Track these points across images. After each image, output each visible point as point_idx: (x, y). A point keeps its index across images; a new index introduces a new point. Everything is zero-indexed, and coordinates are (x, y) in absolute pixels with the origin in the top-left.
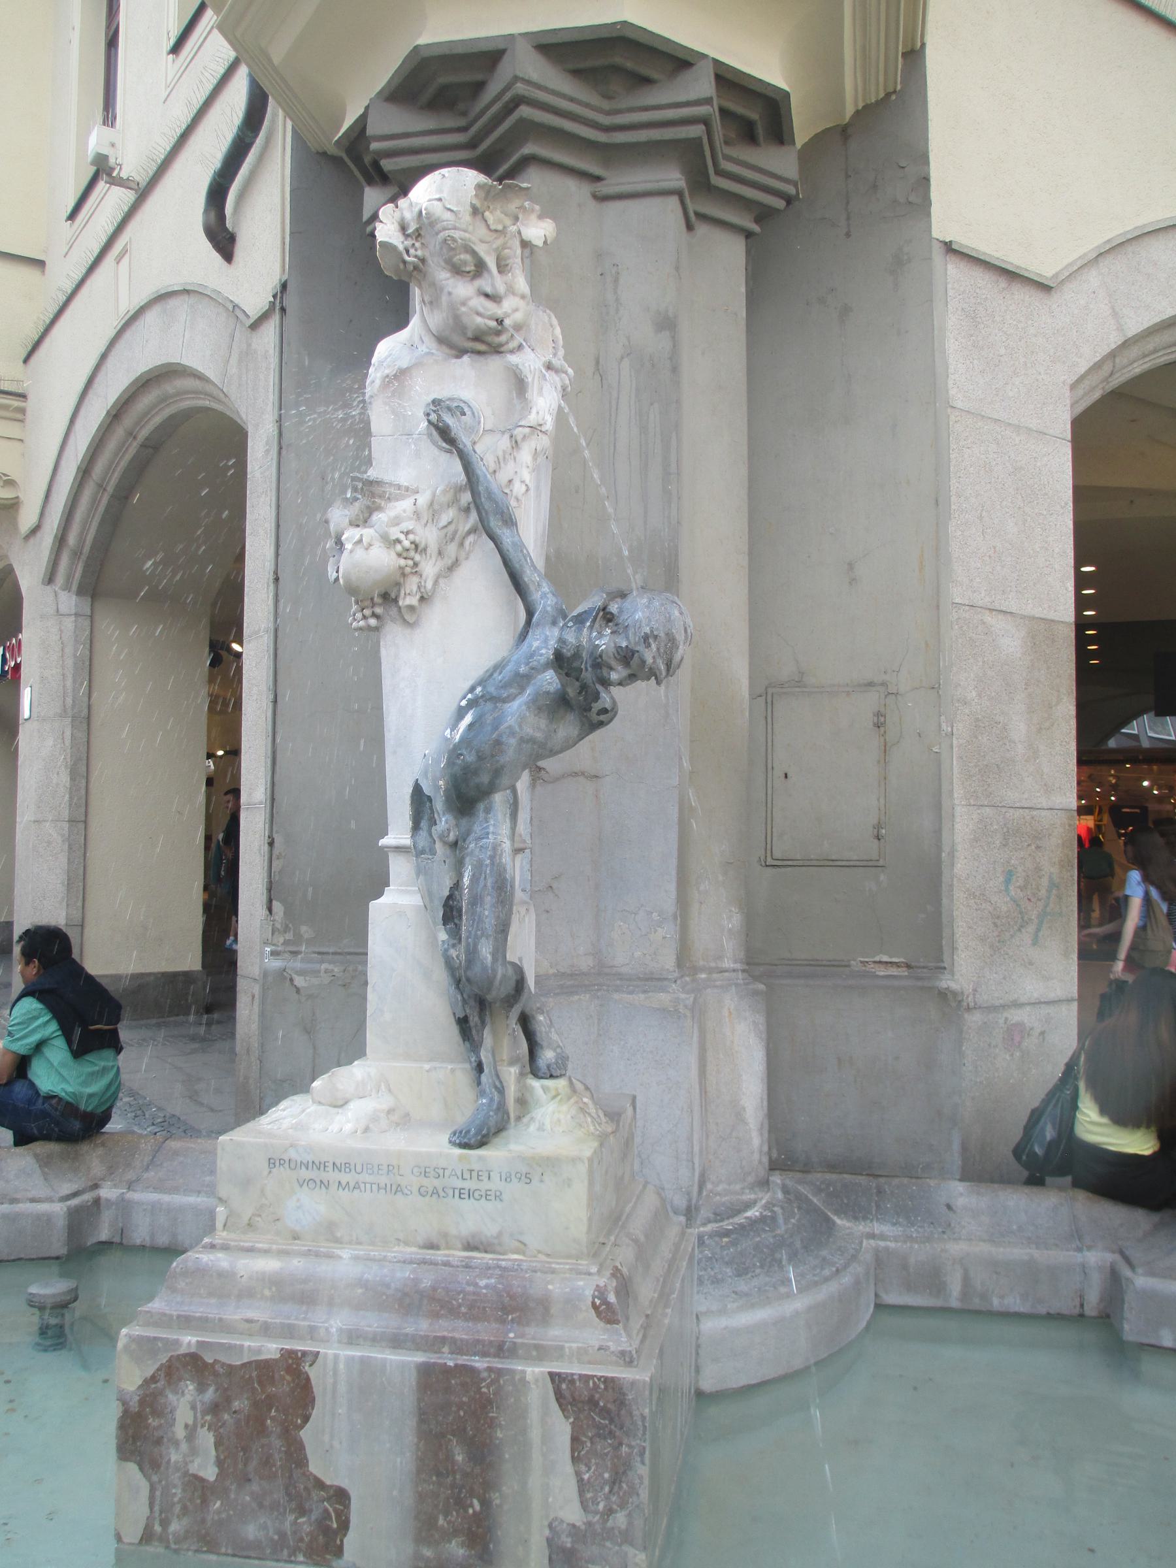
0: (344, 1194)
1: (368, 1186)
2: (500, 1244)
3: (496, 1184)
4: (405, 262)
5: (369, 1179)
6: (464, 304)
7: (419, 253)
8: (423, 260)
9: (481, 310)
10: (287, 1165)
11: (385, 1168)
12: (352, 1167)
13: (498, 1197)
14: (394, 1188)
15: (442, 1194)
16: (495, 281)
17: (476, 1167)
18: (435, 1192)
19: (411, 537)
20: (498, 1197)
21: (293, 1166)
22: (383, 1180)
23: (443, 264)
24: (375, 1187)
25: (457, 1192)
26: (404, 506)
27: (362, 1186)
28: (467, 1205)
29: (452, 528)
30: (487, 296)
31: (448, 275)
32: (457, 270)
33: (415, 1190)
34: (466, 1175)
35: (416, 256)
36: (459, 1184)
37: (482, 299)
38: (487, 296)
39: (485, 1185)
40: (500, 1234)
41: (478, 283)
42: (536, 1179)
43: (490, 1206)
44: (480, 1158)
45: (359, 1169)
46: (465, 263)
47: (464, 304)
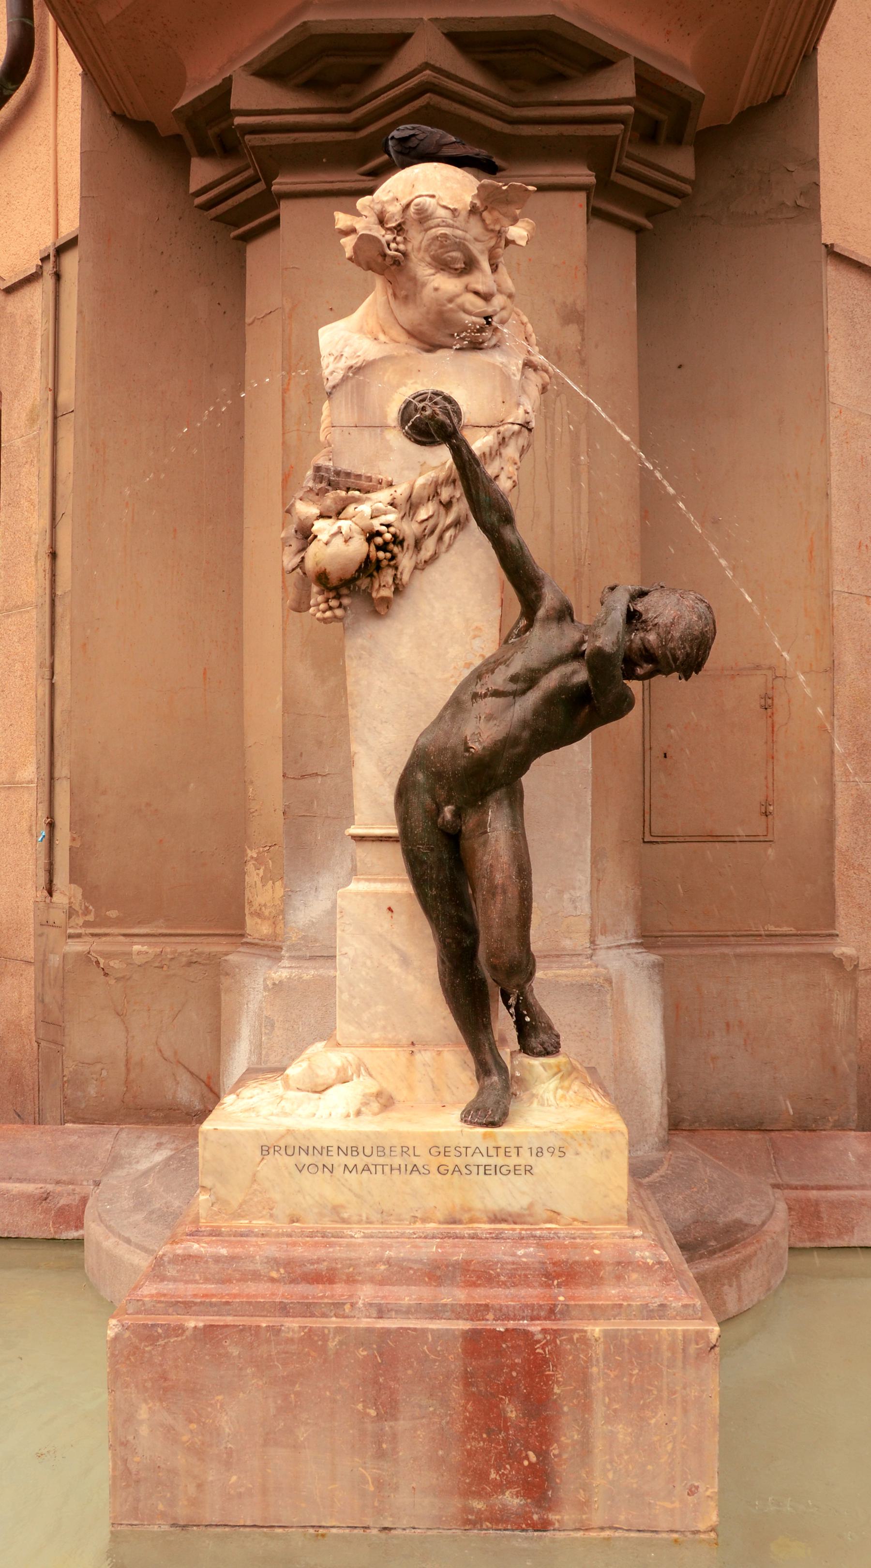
0: (352, 1178)
1: (379, 1168)
2: (531, 1215)
3: (526, 1158)
4: (384, 255)
5: (381, 1160)
6: (450, 301)
7: (402, 247)
8: (405, 254)
9: (468, 306)
10: (283, 1152)
11: (399, 1150)
12: (360, 1150)
13: (529, 1170)
14: (409, 1168)
15: (464, 1171)
16: (482, 279)
17: (503, 1144)
18: (457, 1169)
19: (392, 529)
20: (529, 1170)
21: (290, 1152)
22: (397, 1161)
23: (428, 259)
24: (387, 1169)
25: (482, 1169)
26: (382, 497)
27: (372, 1168)
28: (493, 1182)
29: (431, 523)
30: (477, 293)
31: (432, 271)
32: (443, 265)
33: (434, 1169)
34: (492, 1152)
35: (397, 250)
36: (484, 1161)
37: (471, 297)
38: (477, 293)
39: (513, 1161)
40: (531, 1206)
41: (466, 279)
42: (570, 1154)
43: (520, 1182)
44: (508, 1135)
45: (368, 1151)
46: (454, 260)
47: (450, 301)
